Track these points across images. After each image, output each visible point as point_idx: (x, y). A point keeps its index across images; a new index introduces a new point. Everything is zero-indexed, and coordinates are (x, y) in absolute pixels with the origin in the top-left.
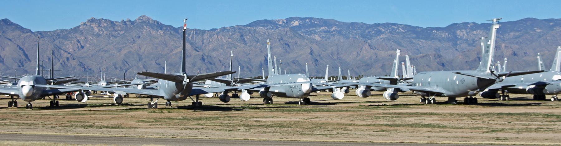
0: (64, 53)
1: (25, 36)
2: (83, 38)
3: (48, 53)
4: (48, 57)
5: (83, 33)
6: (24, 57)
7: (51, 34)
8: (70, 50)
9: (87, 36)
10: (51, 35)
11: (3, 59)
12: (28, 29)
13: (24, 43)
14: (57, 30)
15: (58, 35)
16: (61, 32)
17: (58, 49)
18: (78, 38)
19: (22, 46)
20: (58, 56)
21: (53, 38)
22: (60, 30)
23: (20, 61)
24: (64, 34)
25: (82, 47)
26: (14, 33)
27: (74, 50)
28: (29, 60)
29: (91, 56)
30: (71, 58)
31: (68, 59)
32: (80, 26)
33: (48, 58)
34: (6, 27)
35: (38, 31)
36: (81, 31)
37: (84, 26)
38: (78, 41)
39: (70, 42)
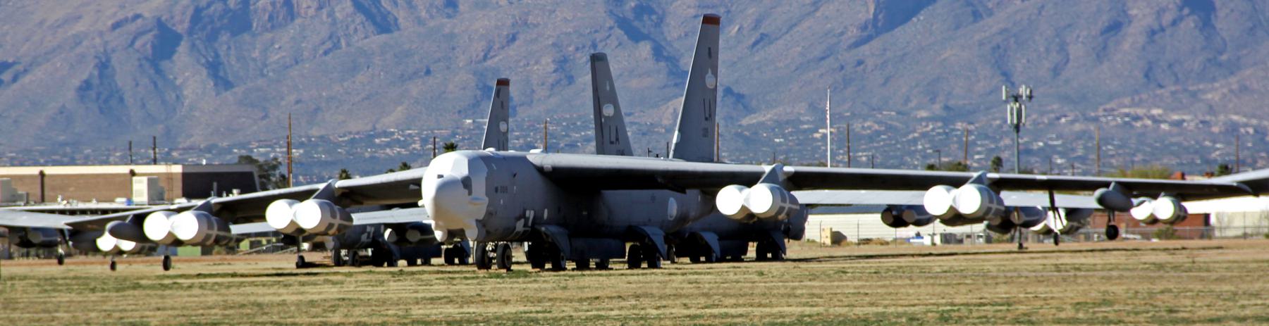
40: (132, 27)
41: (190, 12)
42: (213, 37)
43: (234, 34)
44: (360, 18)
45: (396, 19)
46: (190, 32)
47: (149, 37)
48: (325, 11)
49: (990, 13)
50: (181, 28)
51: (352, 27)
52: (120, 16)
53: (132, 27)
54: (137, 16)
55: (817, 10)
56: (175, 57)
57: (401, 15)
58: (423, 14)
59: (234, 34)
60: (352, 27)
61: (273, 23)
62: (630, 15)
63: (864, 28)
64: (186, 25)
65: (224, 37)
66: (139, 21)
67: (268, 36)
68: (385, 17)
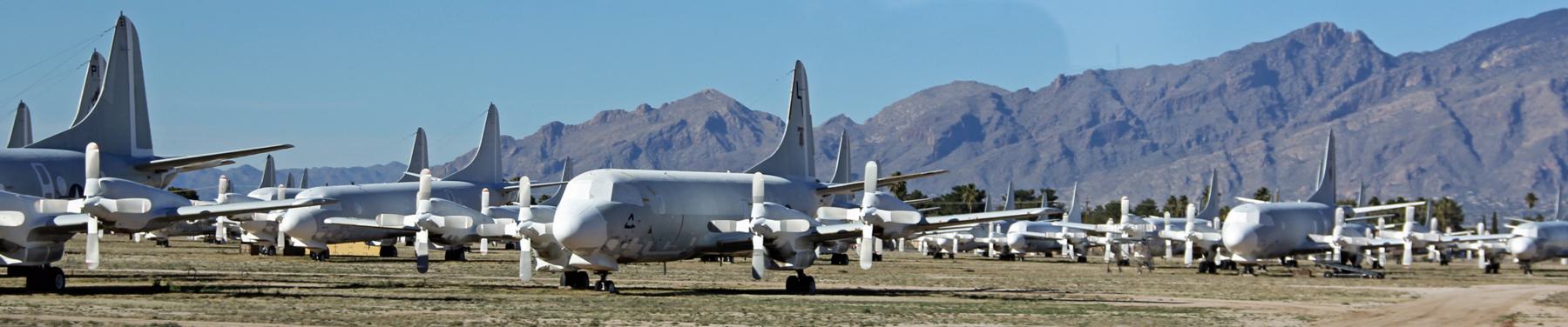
40: (622, 146)
41: (647, 140)
42: (656, 150)
43: (666, 150)
44: (719, 145)
45: (735, 147)
46: (647, 148)
47: (629, 150)
48: (704, 142)
49: (983, 153)
50: (642, 147)
51: (715, 150)
52: (618, 141)
53: (622, 146)
54: (625, 141)
55: (909, 149)
56: (639, 159)
57: (737, 144)
58: (747, 145)
59: (666, 150)
60: (715, 150)
61: (682, 146)
62: (830, 149)
63: (928, 158)
64: (645, 146)
65: (661, 151)
66: (625, 144)
67: (680, 151)
68: (730, 145)
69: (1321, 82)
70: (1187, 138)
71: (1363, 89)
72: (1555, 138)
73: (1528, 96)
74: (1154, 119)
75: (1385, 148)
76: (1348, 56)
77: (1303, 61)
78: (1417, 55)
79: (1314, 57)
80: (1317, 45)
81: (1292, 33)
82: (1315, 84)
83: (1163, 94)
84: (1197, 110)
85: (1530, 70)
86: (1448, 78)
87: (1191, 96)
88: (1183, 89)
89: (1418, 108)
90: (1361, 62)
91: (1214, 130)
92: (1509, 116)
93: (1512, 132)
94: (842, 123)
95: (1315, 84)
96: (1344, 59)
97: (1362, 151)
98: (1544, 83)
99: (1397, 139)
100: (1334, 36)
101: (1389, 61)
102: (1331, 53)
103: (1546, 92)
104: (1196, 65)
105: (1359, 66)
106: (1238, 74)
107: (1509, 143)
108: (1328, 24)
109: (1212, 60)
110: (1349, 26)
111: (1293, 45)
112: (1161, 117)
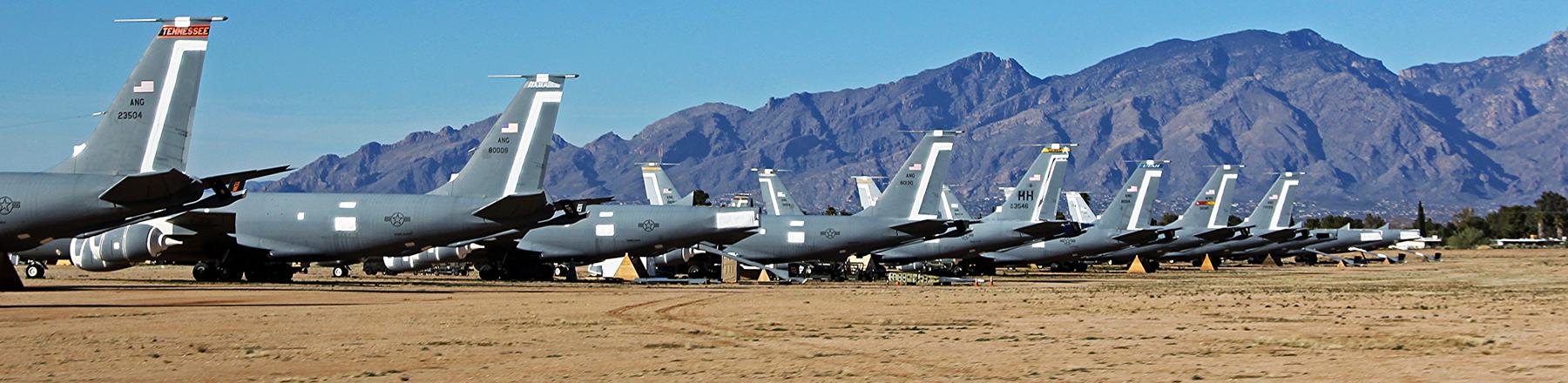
0: (1431, 133)
1: (1331, 81)
2: (1542, 83)
3: (1377, 134)
4: (1373, 146)
5: (1546, 66)
6: (1302, 148)
7: (1464, 72)
8: (1487, 122)
9: (1556, 77)
10: (1460, 75)
11: (1240, 155)
12: (1369, 60)
13: (1320, 106)
14: (1485, 58)
15: (1480, 75)
16: (1491, 66)
17: (1416, 123)
18: (1527, 85)
19: (1311, 115)
20: (1409, 144)
21: (1460, 85)
22: (1488, 59)
23: (1289, 158)
24: (1497, 70)
25: (1531, 111)
26: (1300, 75)
27: (1501, 124)
28: (1321, 155)
29: (1536, 142)
30: (1443, 150)
31: (1431, 153)
32: (1545, 46)
33: (1371, 150)
34: (1290, 56)
35: (1426, 65)
36: (1541, 61)
37: (1557, 43)
38: (1524, 94)
39: (1496, 97)
69: (979, 103)
70: (866, 148)
71: (1004, 107)
72: (1127, 145)
73: (1115, 112)
74: (843, 133)
75: (1002, 154)
76: (1002, 79)
77: (967, 84)
78: (1060, 77)
79: (975, 81)
80: (978, 70)
81: (958, 61)
82: (975, 102)
83: (853, 110)
84: (878, 125)
85: (1130, 90)
86: (1071, 96)
87: (873, 114)
88: (868, 107)
89: (1028, 122)
90: (1012, 84)
91: (888, 141)
92: (1098, 128)
93: (1100, 140)
94: (611, 139)
95: (975, 102)
96: (999, 82)
97: (982, 157)
98: (1128, 101)
99: (1010, 147)
100: (992, 63)
101: (1035, 81)
102: (990, 77)
103: (1129, 108)
104: (880, 88)
105: (1010, 87)
106: (911, 95)
107: (1095, 150)
108: (987, 53)
109: (892, 83)
110: (1004, 56)
111: (959, 71)
112: (848, 131)
